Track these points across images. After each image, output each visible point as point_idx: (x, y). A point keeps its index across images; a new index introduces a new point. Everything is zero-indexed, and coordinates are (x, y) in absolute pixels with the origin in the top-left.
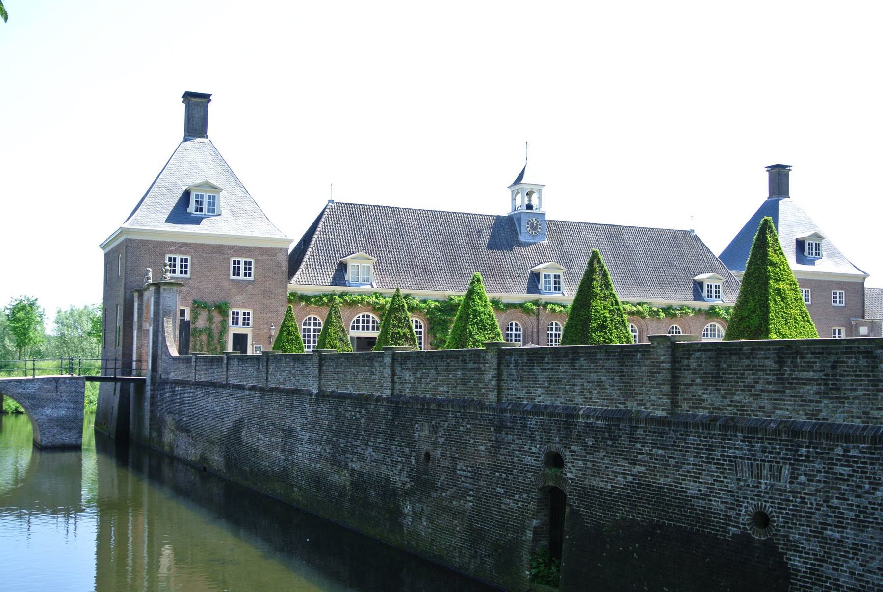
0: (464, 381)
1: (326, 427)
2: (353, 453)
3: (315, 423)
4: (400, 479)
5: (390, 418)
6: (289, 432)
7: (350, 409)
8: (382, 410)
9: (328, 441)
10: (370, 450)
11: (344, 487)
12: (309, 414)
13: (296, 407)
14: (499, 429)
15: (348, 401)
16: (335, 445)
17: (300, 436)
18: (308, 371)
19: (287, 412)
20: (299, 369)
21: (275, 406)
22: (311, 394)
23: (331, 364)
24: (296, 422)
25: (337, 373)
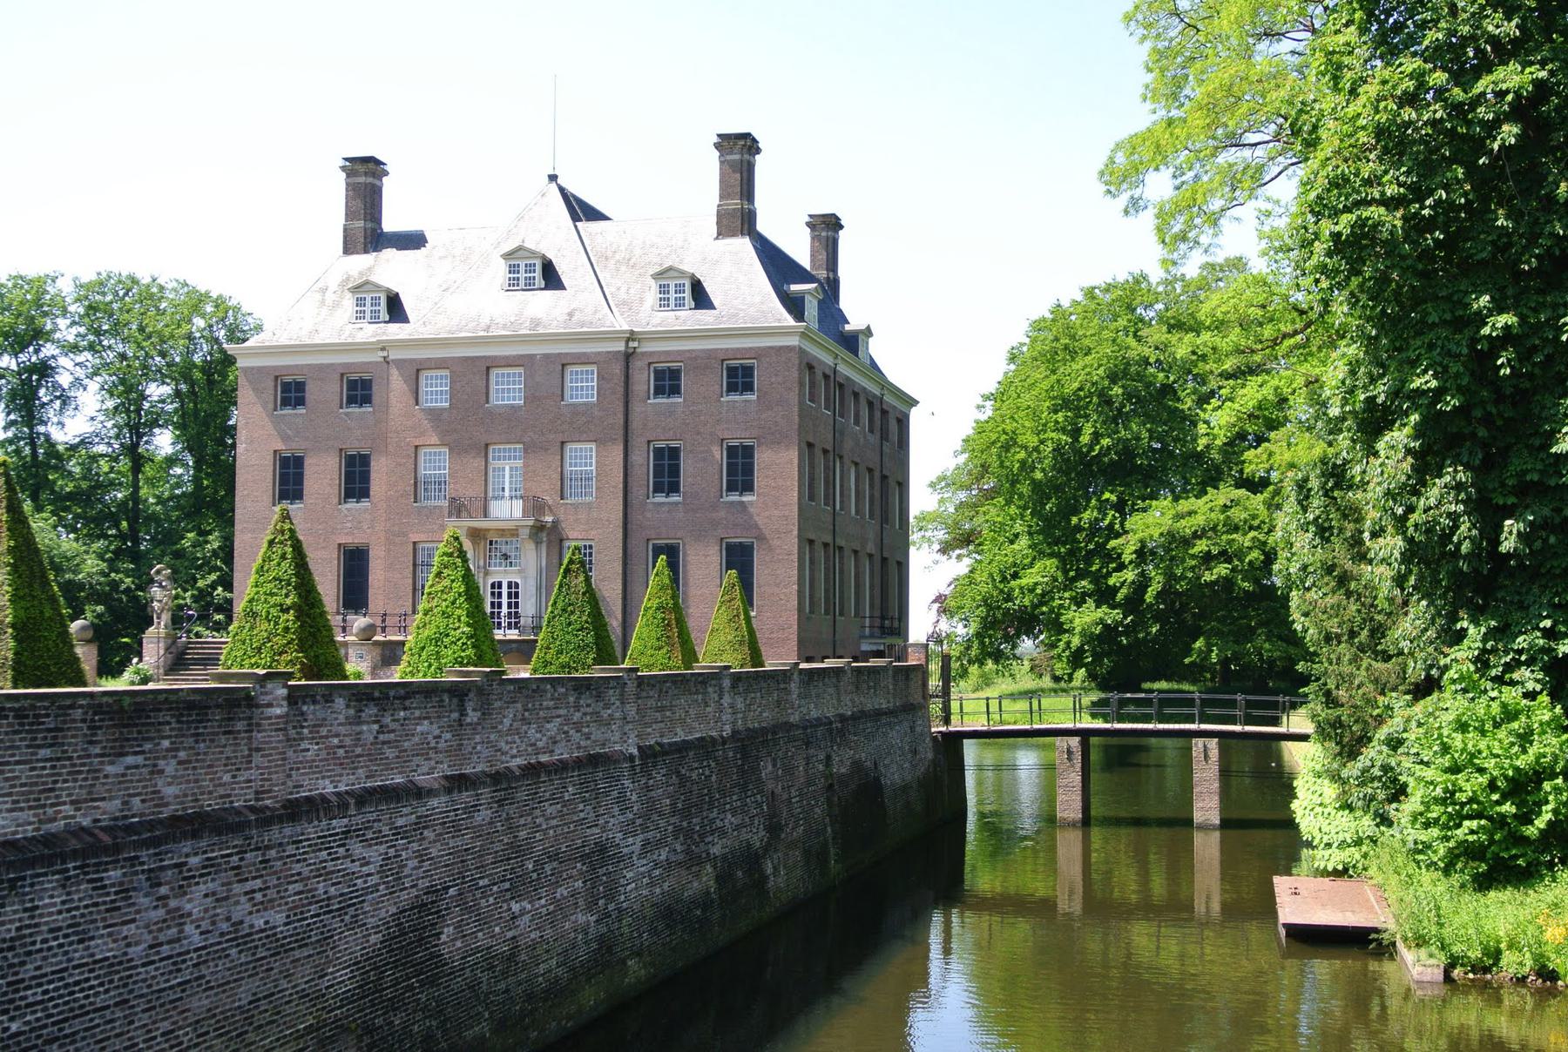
0: (779, 703)
1: (667, 810)
2: (712, 832)
3: (650, 809)
4: (757, 837)
5: (740, 762)
6: (600, 855)
7: (696, 765)
8: (731, 754)
9: (678, 830)
10: (729, 816)
11: (708, 893)
12: (634, 798)
13: (607, 794)
14: (808, 744)
15: (691, 754)
16: (688, 833)
17: (625, 851)
18: (609, 711)
19: (585, 811)
20: (589, 710)
21: (551, 810)
22: (631, 758)
23: (651, 693)
24: (612, 826)
25: (661, 709)
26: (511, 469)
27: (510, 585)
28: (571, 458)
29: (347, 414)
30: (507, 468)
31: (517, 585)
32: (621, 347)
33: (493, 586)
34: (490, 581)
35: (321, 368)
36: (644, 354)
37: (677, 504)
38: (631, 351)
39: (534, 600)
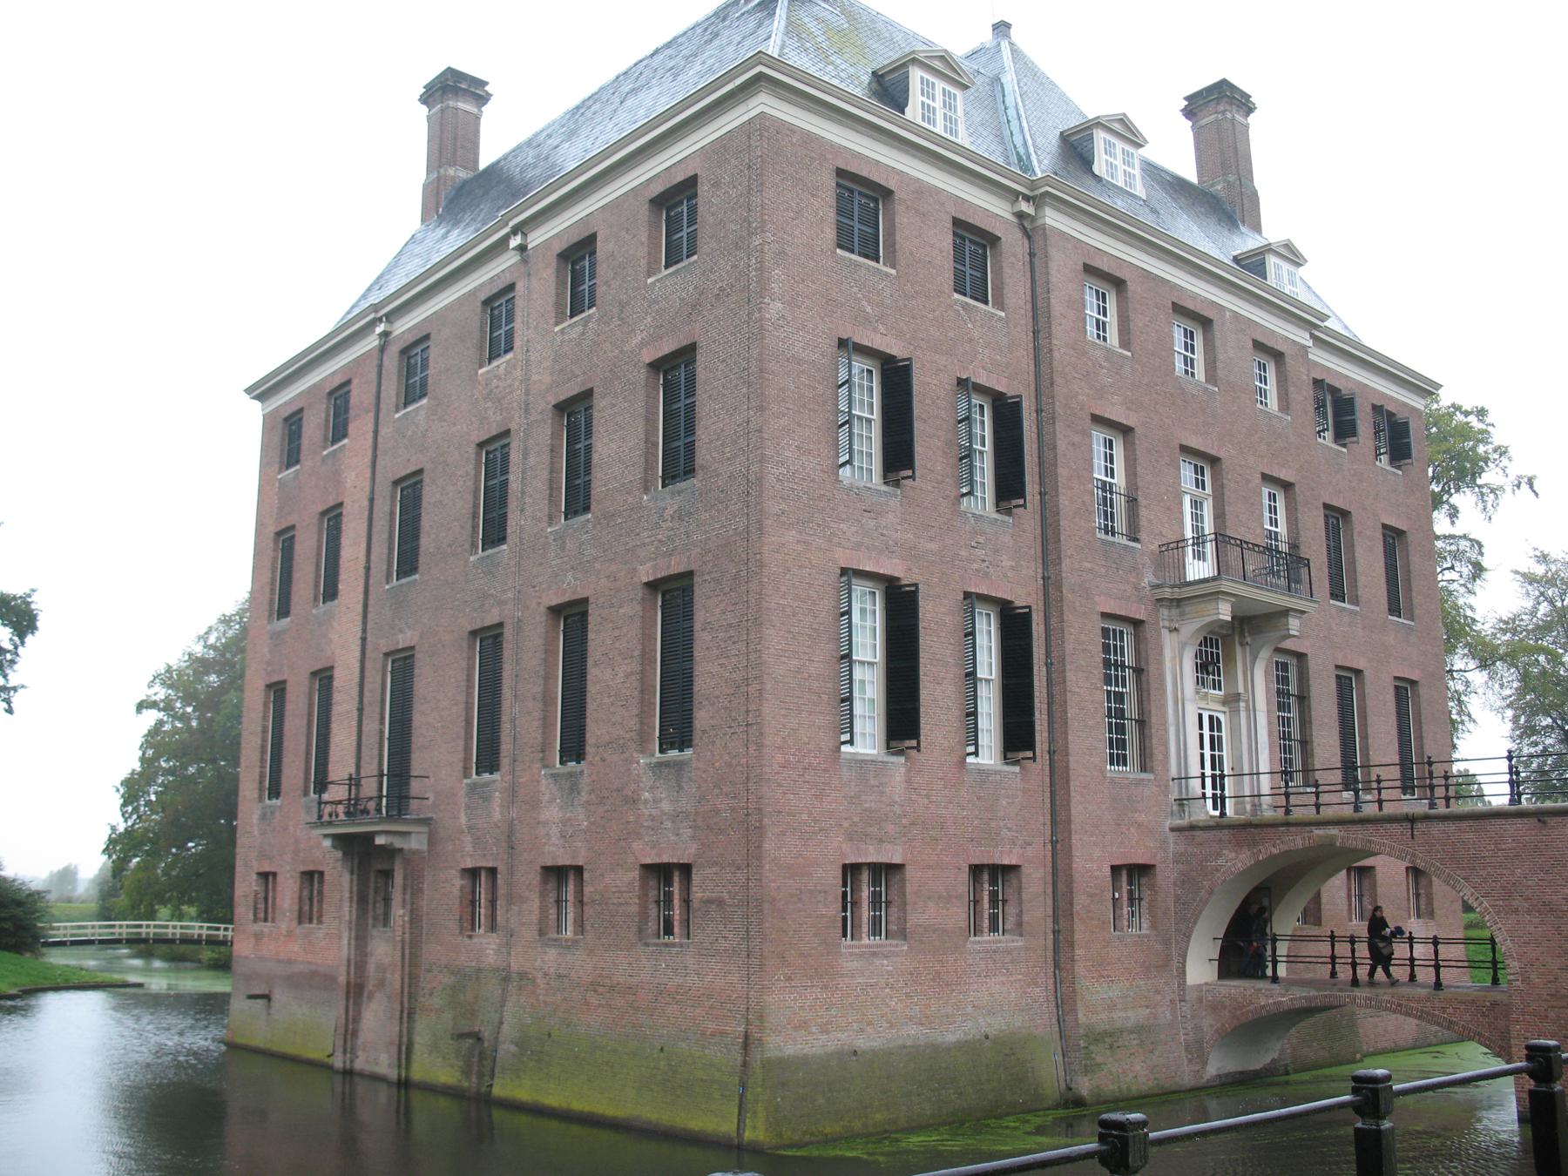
27: (1211, 718)
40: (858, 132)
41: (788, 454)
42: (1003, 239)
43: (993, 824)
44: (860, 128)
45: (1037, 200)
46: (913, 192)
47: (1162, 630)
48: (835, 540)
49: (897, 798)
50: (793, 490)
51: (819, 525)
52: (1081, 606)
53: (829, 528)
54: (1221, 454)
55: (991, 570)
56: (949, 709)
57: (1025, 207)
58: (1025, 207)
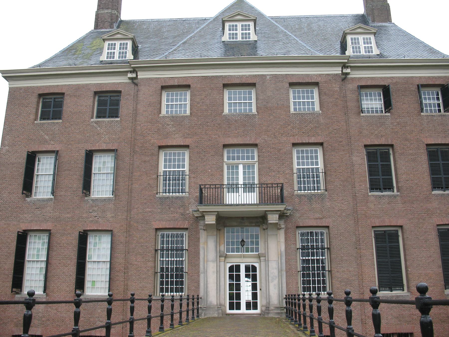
26: (244, 168)
28: (298, 158)
29: (96, 123)
30: (241, 167)
31: (254, 269)
32: (337, 71)
33: (231, 269)
34: (229, 265)
35: (78, 87)
36: (353, 79)
37: (395, 196)
38: (344, 77)
39: (276, 282)
40: (48, 79)
41: (4, 195)
42: (123, 91)
43: (92, 319)
44: (48, 77)
45: (134, 71)
46: (74, 90)
47: (201, 231)
48: (21, 221)
49: (40, 311)
50: (5, 207)
51: (15, 217)
52: (142, 227)
53: (19, 217)
54: (257, 142)
55: (100, 220)
56: (71, 275)
57: (130, 75)
58: (130, 75)
